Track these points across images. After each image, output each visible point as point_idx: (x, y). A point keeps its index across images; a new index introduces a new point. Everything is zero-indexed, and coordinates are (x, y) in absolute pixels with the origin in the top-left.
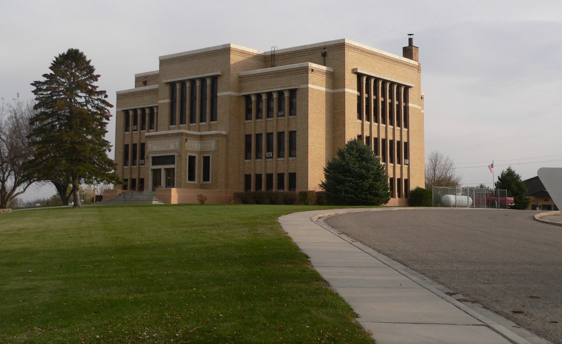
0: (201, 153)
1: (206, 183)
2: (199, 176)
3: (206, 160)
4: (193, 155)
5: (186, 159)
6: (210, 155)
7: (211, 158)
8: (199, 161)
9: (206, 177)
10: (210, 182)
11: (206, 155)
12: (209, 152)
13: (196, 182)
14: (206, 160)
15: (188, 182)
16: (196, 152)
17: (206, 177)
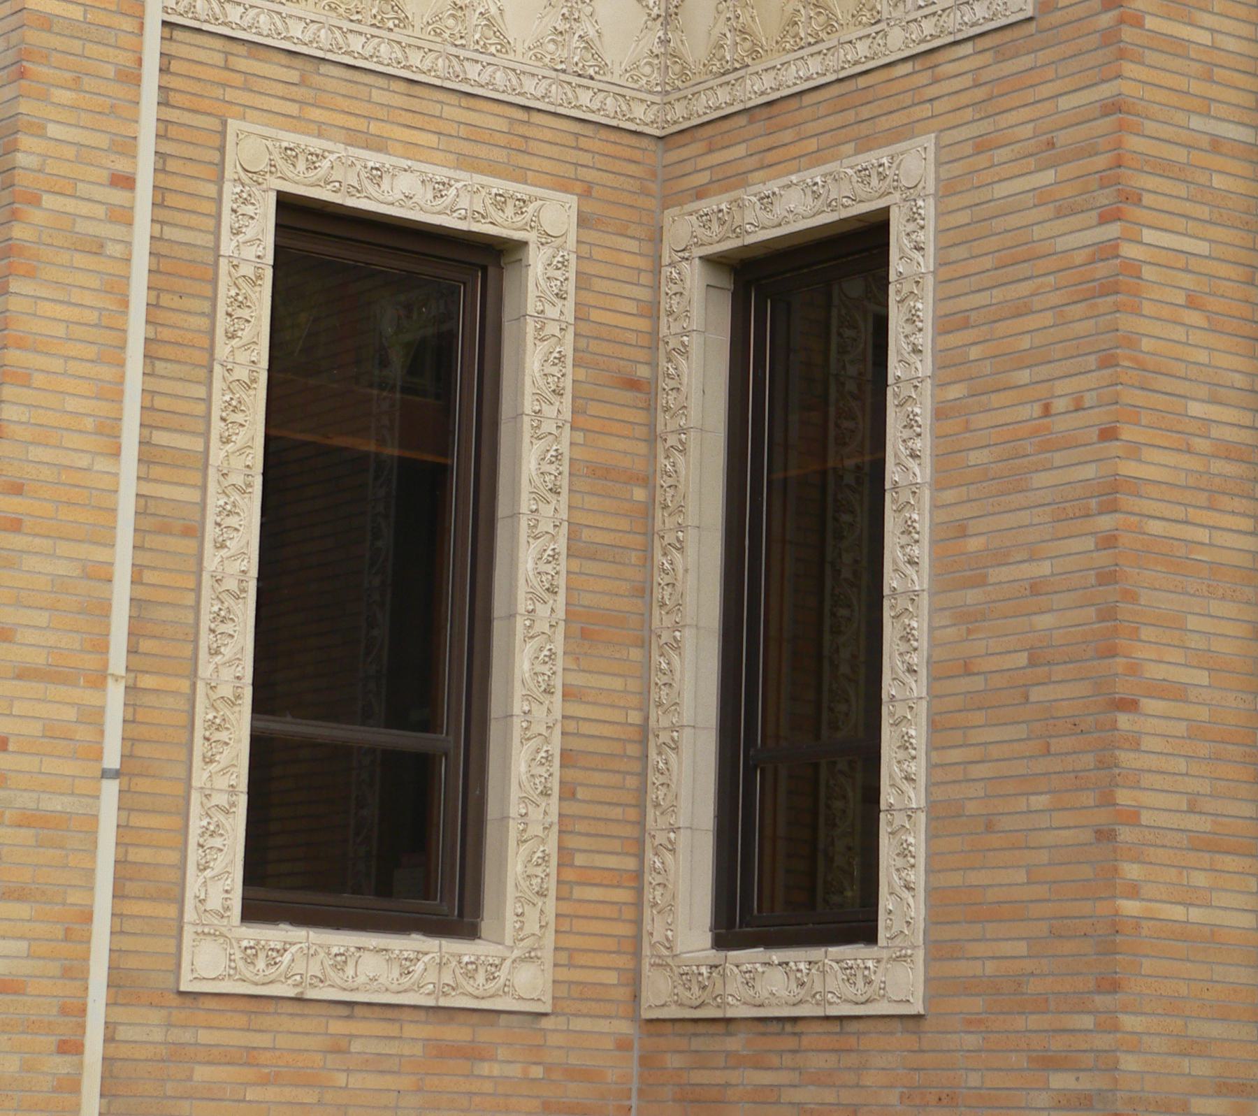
0: (683, 151)
1: (775, 978)
2: (607, 773)
3: (809, 314)
4: (407, 188)
5: (183, 274)
6: (902, 179)
7: (911, 261)
8: (623, 382)
9: (797, 851)
10: (886, 974)
11: (792, 203)
12: (854, 105)
13: (511, 958)
14: (809, 314)
15: (224, 947)
16: (514, 131)
17: (797, 851)
